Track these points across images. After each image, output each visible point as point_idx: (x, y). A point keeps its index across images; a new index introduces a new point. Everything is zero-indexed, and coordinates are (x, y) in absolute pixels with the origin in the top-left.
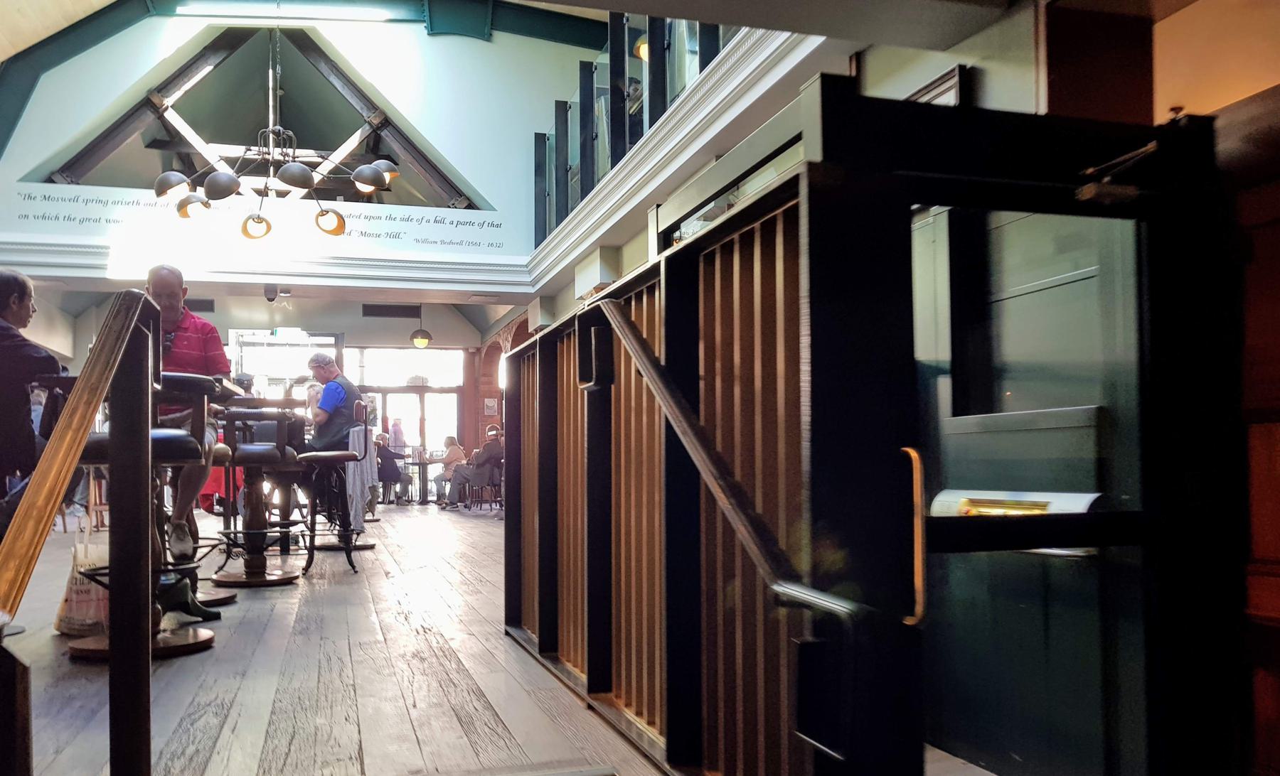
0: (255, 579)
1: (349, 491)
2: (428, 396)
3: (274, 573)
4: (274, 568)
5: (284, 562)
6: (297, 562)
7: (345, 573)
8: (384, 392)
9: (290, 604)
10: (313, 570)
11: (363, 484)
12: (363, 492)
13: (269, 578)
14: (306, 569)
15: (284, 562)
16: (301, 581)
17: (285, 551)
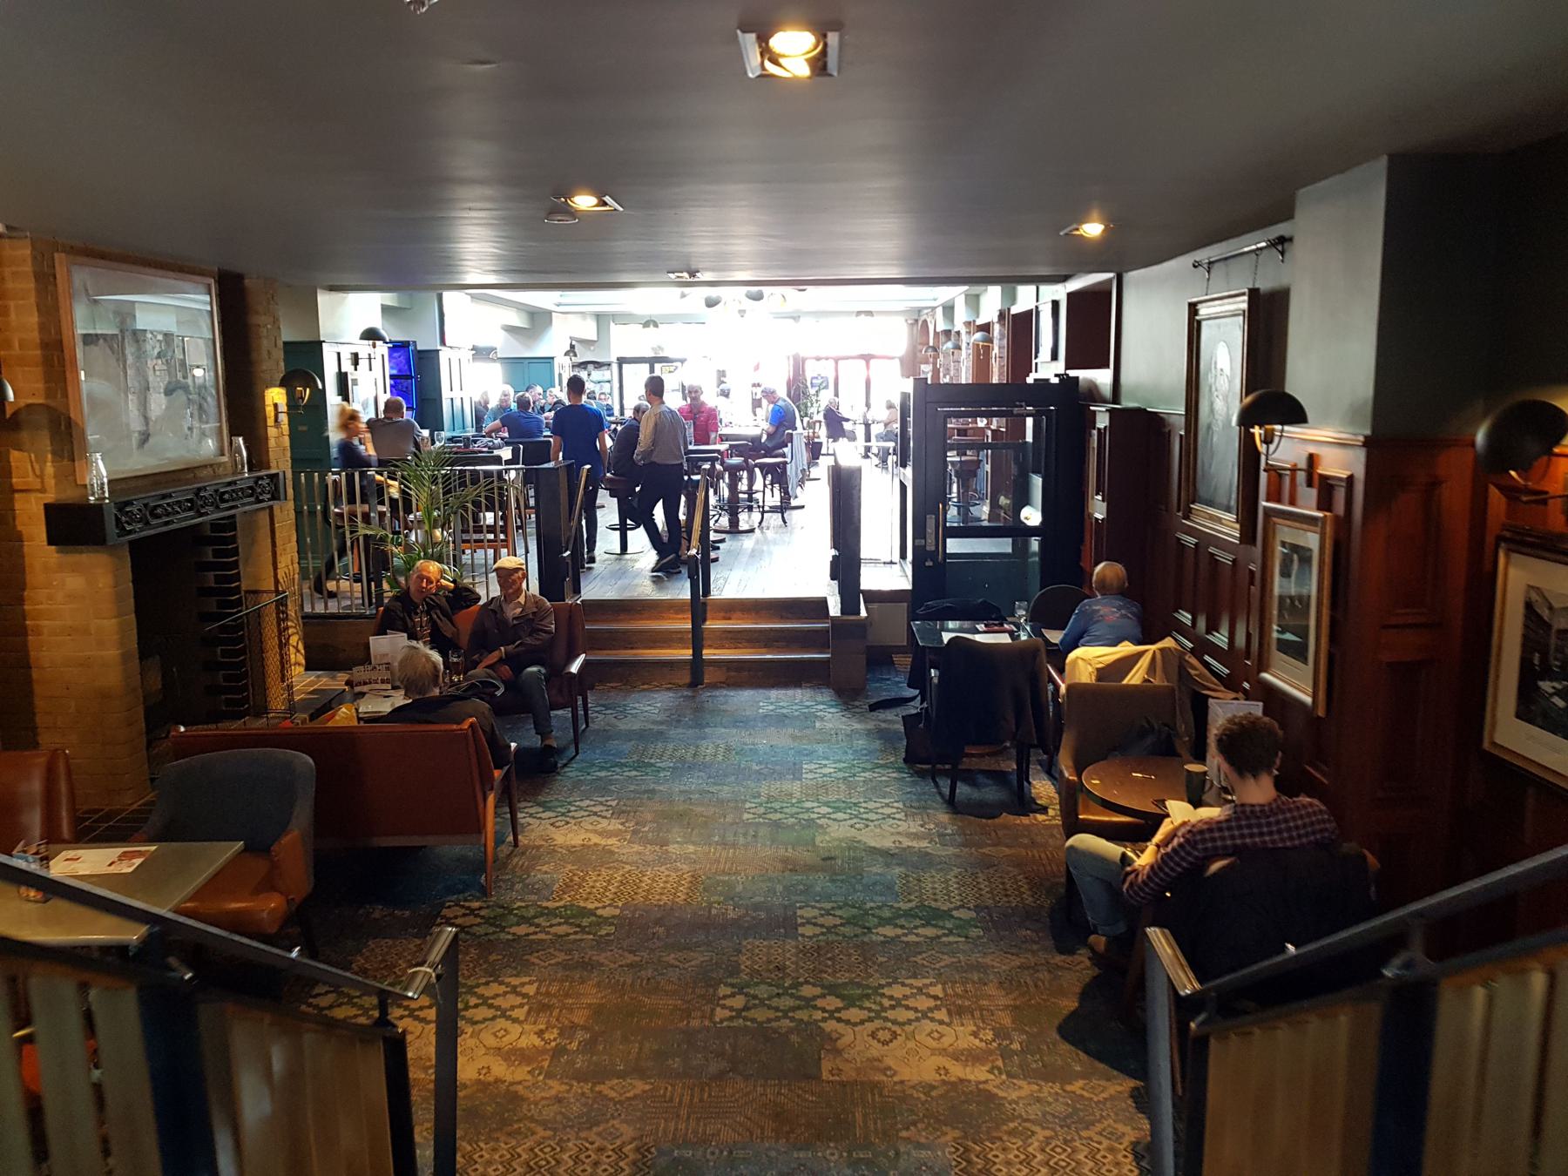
0: (734, 529)
1: (788, 473)
2: (872, 362)
3: (743, 526)
4: (745, 521)
5: (750, 517)
6: (756, 516)
7: (781, 526)
8: (837, 360)
9: (748, 542)
10: (764, 524)
11: (797, 468)
12: (796, 474)
13: (740, 529)
14: (760, 523)
15: (750, 517)
16: (757, 531)
17: (750, 509)
